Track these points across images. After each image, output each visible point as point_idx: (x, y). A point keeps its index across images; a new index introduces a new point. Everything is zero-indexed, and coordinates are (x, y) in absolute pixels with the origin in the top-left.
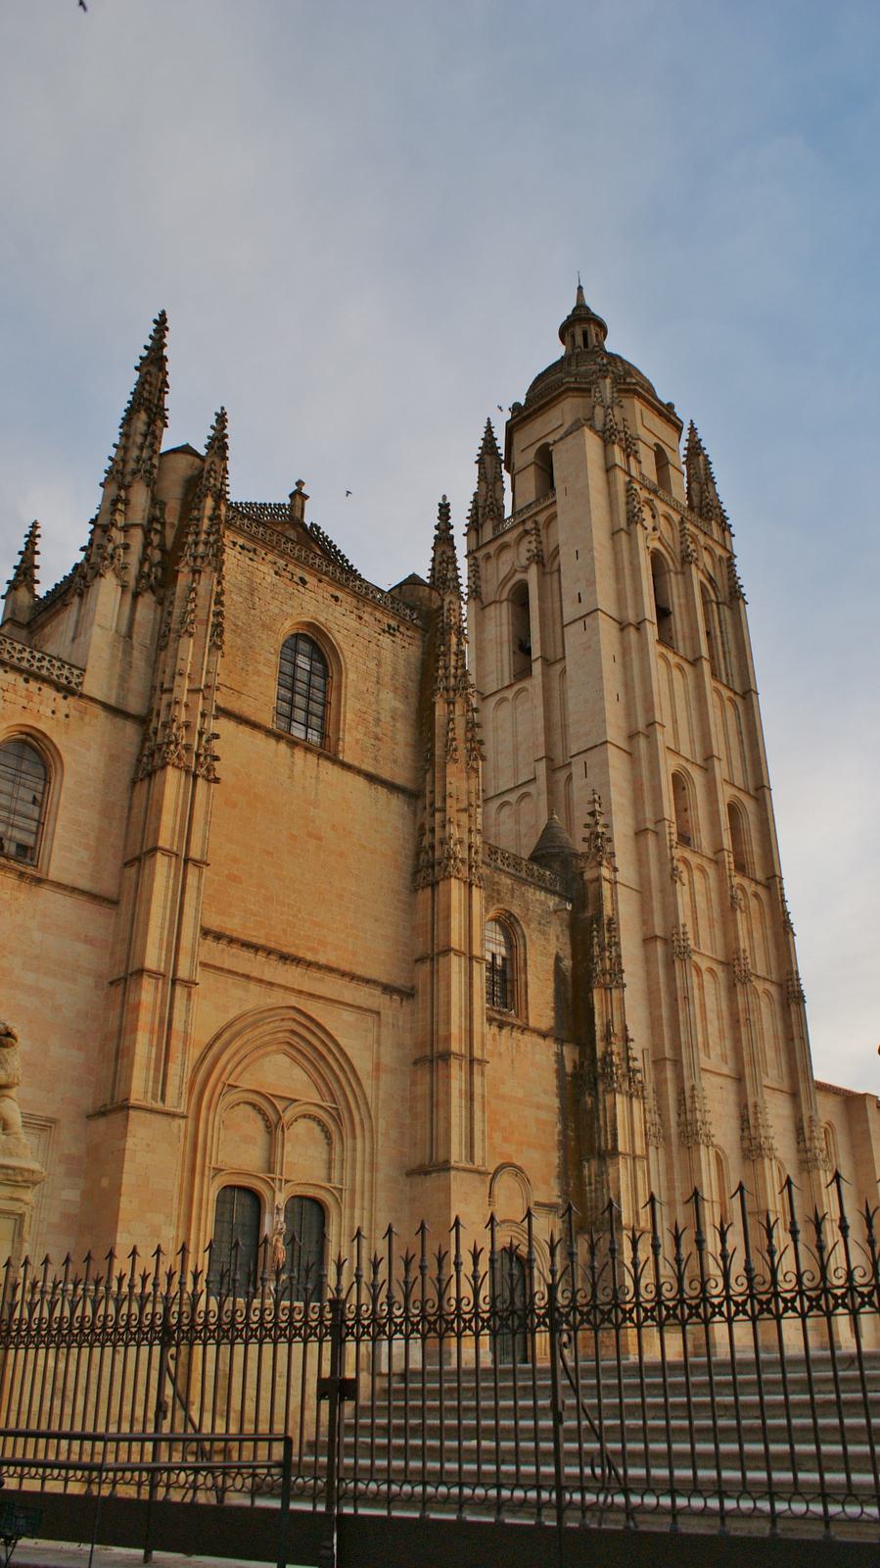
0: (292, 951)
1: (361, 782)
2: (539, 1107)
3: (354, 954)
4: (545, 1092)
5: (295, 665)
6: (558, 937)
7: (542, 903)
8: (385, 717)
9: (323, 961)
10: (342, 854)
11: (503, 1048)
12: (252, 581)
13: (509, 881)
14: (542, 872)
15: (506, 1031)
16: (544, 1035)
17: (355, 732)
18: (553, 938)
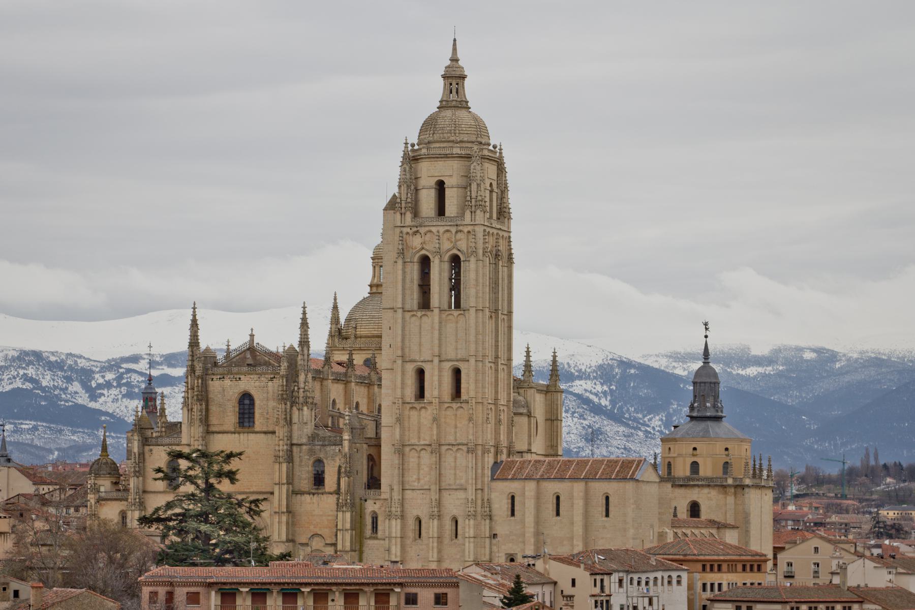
0: (242, 490)
1: (263, 435)
2: (329, 516)
3: (262, 486)
4: (332, 511)
5: (244, 404)
6: (340, 460)
7: (333, 450)
8: (270, 410)
9: (252, 490)
10: (257, 459)
11: (314, 501)
12: (223, 388)
13: (319, 447)
14: (335, 438)
15: (315, 496)
16: (331, 493)
17: (260, 421)
18: (338, 461)
